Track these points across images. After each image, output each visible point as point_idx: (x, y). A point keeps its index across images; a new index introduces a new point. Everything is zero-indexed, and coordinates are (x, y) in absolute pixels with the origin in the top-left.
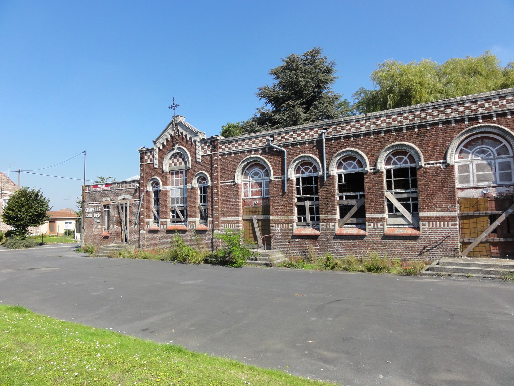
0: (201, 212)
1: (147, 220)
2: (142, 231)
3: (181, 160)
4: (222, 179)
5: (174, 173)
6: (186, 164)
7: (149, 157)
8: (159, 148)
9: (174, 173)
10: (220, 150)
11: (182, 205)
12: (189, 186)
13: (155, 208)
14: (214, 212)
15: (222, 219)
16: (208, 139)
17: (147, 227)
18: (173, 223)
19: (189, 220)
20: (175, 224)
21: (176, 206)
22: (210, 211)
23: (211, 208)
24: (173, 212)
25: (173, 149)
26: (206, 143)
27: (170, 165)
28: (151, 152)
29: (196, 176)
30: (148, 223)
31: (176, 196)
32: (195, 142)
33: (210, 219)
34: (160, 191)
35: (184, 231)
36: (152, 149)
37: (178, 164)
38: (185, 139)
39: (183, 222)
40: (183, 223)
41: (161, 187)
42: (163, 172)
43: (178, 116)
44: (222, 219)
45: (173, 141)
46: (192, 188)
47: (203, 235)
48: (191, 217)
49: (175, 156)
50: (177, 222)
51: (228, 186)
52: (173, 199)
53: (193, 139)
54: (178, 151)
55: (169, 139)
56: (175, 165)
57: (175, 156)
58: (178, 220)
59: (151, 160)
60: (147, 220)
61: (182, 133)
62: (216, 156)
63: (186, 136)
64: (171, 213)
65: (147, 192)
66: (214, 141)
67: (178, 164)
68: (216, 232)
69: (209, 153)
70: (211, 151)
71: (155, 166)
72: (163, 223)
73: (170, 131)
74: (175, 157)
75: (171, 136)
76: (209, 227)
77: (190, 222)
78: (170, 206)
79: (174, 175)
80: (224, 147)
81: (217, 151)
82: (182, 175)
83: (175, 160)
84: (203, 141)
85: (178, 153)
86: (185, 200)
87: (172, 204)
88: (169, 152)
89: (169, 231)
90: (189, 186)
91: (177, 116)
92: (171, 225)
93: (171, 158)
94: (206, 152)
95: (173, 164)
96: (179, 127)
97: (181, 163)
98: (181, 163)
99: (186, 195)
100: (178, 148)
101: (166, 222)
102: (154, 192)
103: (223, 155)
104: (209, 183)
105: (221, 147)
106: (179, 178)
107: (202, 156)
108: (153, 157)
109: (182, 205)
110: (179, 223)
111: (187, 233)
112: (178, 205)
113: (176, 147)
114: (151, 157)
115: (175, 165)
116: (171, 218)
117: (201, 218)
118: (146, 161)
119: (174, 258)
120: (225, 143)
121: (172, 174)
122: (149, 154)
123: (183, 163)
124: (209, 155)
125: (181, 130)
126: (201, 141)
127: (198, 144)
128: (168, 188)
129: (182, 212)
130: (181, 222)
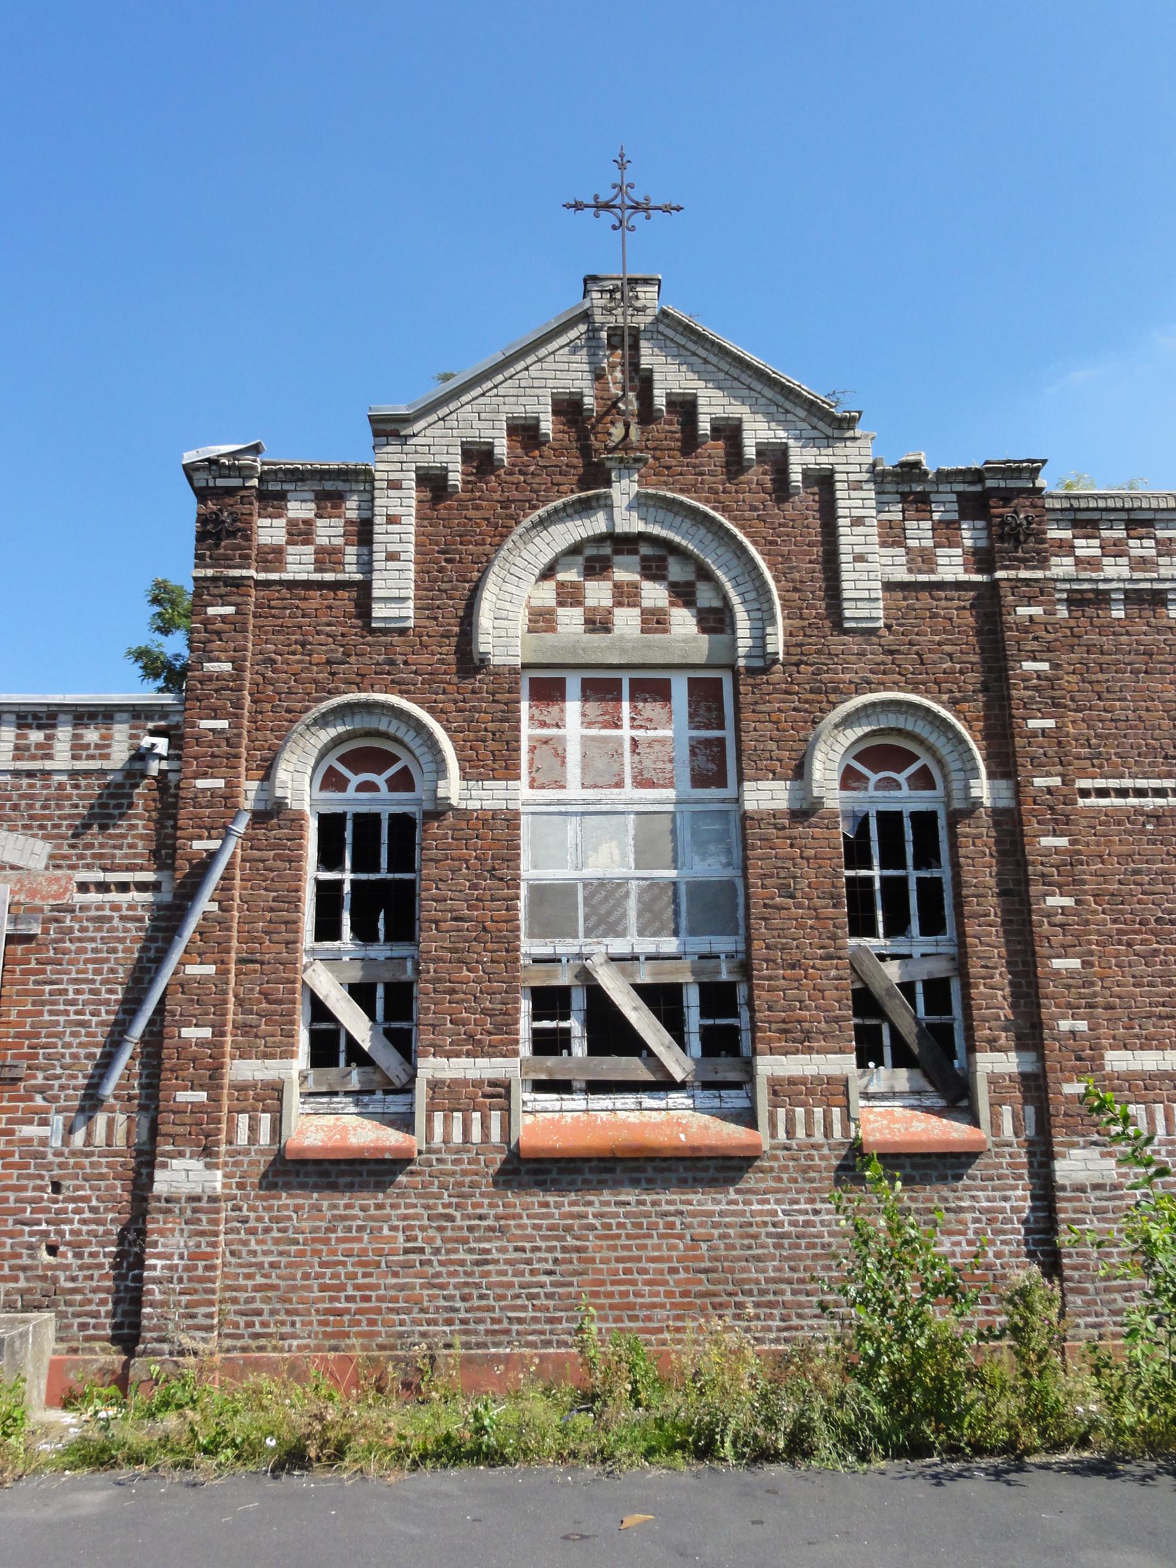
0: (865, 1002)
1: (243, 1070)
2: (180, 1175)
3: (655, 594)
4: (1097, 763)
5: (573, 684)
6: (716, 621)
7: (301, 533)
8: (433, 483)
9: (573, 684)
10: (1062, 567)
11: (670, 945)
12: (767, 795)
13: (332, 960)
14: (1049, 1010)
15: (1117, 1061)
16: (944, 476)
17: (247, 1133)
18: (548, 1100)
19: (768, 1066)
20: (577, 1101)
21: (599, 949)
22: (993, 996)
23: (1001, 977)
24: (550, 1001)
25: (584, 508)
26: (919, 503)
27: (542, 620)
28: (328, 500)
29: (848, 721)
30: (271, 1096)
31: (594, 871)
32: (823, 481)
33: (995, 1064)
34: (439, 811)
35: (721, 1168)
36: (362, 477)
37: (627, 621)
38: (717, 449)
39: (681, 1086)
40: (677, 1098)
41: (453, 788)
42: (469, 662)
43: (646, 281)
44: (1117, 1061)
45: (586, 451)
46: (805, 812)
47: (931, 1194)
48: (800, 1039)
49: (596, 557)
50: (596, 1087)
51: (1156, 816)
52: (540, 892)
53: (802, 459)
54: (636, 525)
55: (547, 426)
56: (598, 623)
57: (596, 557)
58: (633, 1068)
59: (327, 557)
60: (243, 1070)
61: (685, 407)
62: (1030, 601)
63: (729, 432)
64: (526, 1006)
65: (271, 813)
66: (1007, 496)
67: (627, 621)
68: (1075, 1165)
69: (952, 566)
70: (983, 560)
71: (378, 611)
72: (448, 1096)
73: (568, 371)
74: (596, 568)
75: (568, 408)
76: (1001, 1126)
77: (781, 1089)
78: (529, 947)
79: (573, 708)
80: (1087, 548)
81: (1043, 564)
82: (652, 709)
83: (598, 593)
84: (905, 484)
85: (625, 543)
86: (714, 907)
87: (541, 930)
88: (543, 523)
89: (528, 1170)
90: (767, 795)
91: (633, 282)
92: (552, 1121)
93: (548, 573)
94: (926, 559)
95: (571, 620)
96: (649, 357)
97: (655, 621)
98: (655, 621)
99: (710, 867)
100: (641, 503)
101: (501, 1091)
102: (330, 825)
103: (1088, 600)
104: (983, 789)
105: (1065, 548)
106: (626, 732)
107: (889, 586)
108: (363, 533)
109: (670, 945)
110: (627, 1100)
111: (751, 1180)
112: (619, 946)
113: (624, 490)
114: (329, 532)
115: (598, 623)
116: (525, 1049)
117: (868, 1053)
118: (273, 557)
119: (918, 1418)
120: (1094, 524)
121: (548, 691)
122: (299, 509)
123: (683, 622)
124: (958, 585)
125: (670, 377)
126: (878, 476)
127: (855, 502)
128: (520, 793)
129: (663, 1000)
130: (665, 1084)
